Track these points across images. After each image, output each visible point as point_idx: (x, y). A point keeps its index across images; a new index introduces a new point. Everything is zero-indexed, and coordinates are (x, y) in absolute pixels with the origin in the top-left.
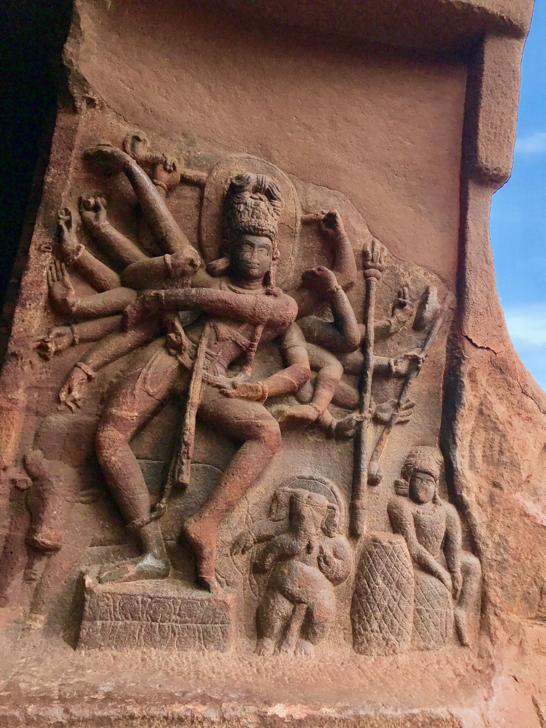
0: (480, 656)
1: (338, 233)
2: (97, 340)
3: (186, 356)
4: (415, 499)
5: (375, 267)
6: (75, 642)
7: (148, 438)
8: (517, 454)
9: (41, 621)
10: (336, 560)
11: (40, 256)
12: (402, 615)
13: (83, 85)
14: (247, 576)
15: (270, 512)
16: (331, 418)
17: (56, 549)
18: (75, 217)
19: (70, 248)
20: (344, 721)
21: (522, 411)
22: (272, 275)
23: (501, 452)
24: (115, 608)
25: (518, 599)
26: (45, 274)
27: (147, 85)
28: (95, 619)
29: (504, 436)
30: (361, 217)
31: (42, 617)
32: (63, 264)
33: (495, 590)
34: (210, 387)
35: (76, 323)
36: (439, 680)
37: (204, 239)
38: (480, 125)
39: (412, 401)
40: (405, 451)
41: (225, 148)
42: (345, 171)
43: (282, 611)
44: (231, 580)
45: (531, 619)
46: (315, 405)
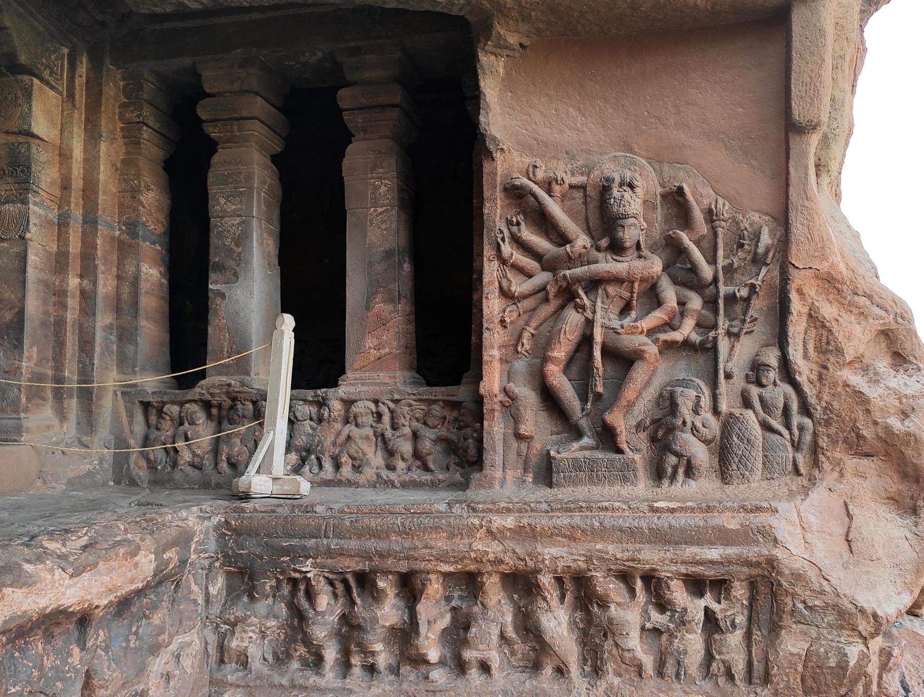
0: (810, 480)
1: (687, 201)
3: (589, 311)
4: (761, 385)
6: (550, 485)
7: (575, 368)
15: (658, 404)
16: (696, 338)
17: (532, 438)
18: (506, 234)
21: (853, 309)
23: (828, 343)
25: (840, 443)
29: (830, 331)
35: (519, 301)
38: (792, 86)
39: (755, 316)
40: (753, 351)
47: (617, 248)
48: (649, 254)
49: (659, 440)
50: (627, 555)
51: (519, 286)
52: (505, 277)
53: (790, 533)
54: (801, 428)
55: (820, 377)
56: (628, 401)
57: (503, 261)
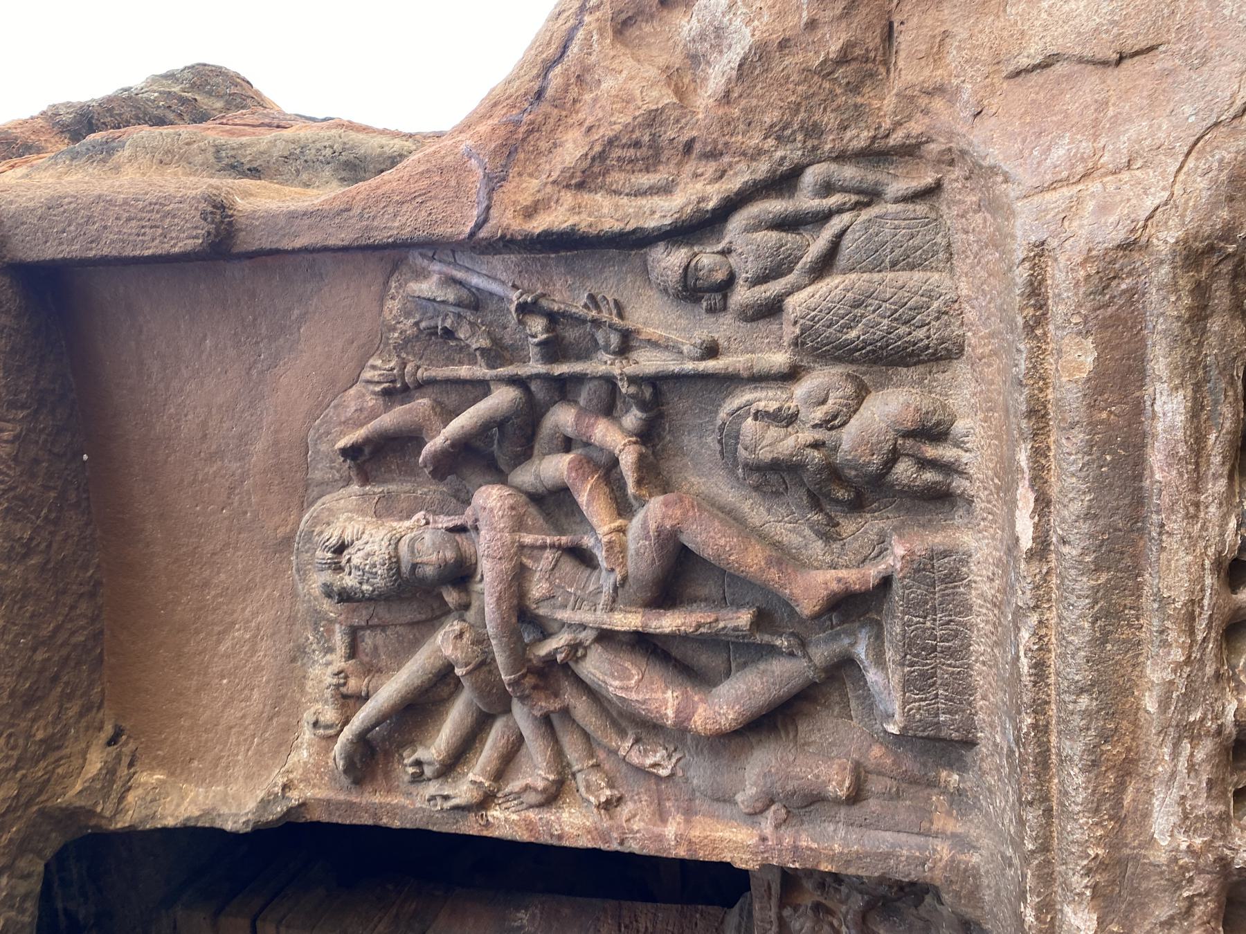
0: (952, 163)
1: (367, 441)
2: (586, 736)
3: (582, 635)
4: (729, 283)
5: (403, 376)
7: (704, 659)
8: (635, 118)
9: (949, 776)
10: (830, 401)
11: (493, 825)
12: (900, 293)
13: (269, 801)
14: (868, 516)
15: (777, 494)
16: (633, 418)
18: (432, 788)
19: (475, 794)
20: (1036, 434)
21: (570, 97)
22: (451, 525)
23: (637, 144)
24: (921, 700)
25: (859, 100)
26: (514, 817)
27: (244, 717)
28: (938, 723)
29: (611, 142)
30: (335, 402)
31: (944, 774)
32: (500, 795)
33: (850, 140)
34: (619, 600)
35: (569, 765)
36: (987, 246)
37: (424, 617)
39: (584, 298)
41: (293, 604)
42: (276, 432)
43: (909, 473)
44: (876, 538)
45: (888, 71)
46: (617, 452)
47: (461, 574)
48: (469, 511)
49: (859, 495)
50: (1174, 634)
51: (535, 772)
52: (518, 795)
53: (1103, 209)
54: (827, 188)
55: (713, 155)
56: (769, 562)
57: (486, 801)
